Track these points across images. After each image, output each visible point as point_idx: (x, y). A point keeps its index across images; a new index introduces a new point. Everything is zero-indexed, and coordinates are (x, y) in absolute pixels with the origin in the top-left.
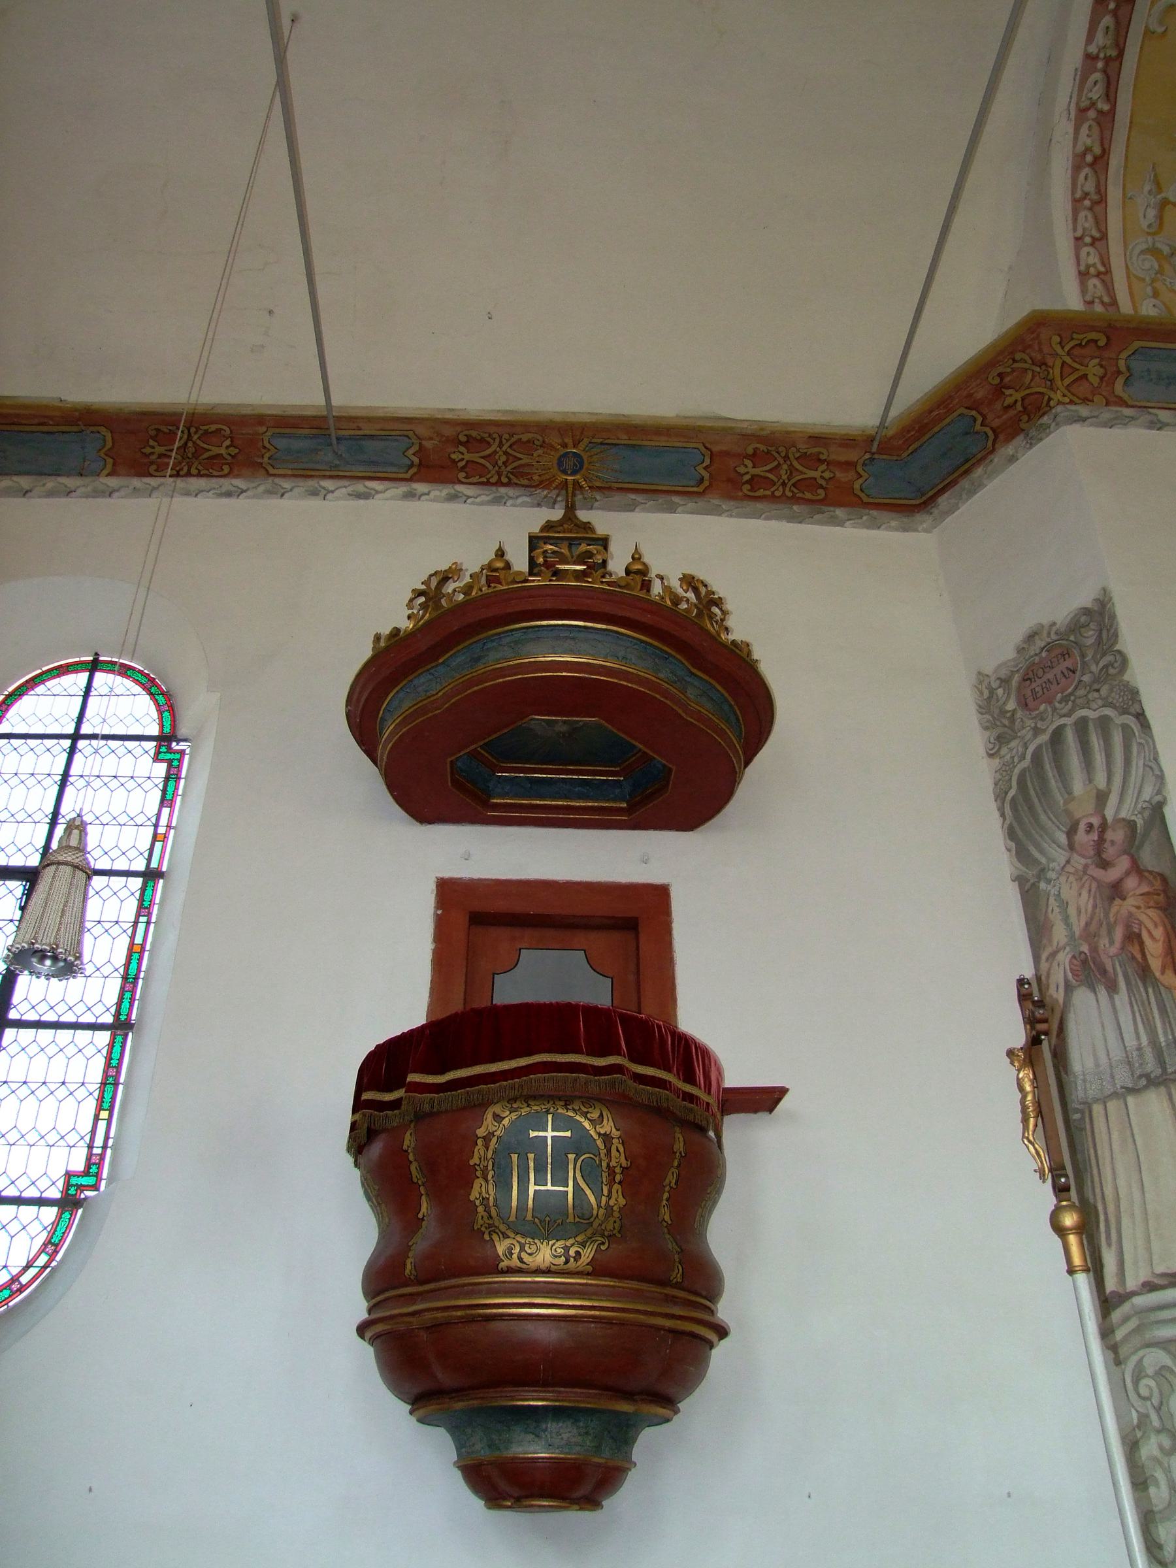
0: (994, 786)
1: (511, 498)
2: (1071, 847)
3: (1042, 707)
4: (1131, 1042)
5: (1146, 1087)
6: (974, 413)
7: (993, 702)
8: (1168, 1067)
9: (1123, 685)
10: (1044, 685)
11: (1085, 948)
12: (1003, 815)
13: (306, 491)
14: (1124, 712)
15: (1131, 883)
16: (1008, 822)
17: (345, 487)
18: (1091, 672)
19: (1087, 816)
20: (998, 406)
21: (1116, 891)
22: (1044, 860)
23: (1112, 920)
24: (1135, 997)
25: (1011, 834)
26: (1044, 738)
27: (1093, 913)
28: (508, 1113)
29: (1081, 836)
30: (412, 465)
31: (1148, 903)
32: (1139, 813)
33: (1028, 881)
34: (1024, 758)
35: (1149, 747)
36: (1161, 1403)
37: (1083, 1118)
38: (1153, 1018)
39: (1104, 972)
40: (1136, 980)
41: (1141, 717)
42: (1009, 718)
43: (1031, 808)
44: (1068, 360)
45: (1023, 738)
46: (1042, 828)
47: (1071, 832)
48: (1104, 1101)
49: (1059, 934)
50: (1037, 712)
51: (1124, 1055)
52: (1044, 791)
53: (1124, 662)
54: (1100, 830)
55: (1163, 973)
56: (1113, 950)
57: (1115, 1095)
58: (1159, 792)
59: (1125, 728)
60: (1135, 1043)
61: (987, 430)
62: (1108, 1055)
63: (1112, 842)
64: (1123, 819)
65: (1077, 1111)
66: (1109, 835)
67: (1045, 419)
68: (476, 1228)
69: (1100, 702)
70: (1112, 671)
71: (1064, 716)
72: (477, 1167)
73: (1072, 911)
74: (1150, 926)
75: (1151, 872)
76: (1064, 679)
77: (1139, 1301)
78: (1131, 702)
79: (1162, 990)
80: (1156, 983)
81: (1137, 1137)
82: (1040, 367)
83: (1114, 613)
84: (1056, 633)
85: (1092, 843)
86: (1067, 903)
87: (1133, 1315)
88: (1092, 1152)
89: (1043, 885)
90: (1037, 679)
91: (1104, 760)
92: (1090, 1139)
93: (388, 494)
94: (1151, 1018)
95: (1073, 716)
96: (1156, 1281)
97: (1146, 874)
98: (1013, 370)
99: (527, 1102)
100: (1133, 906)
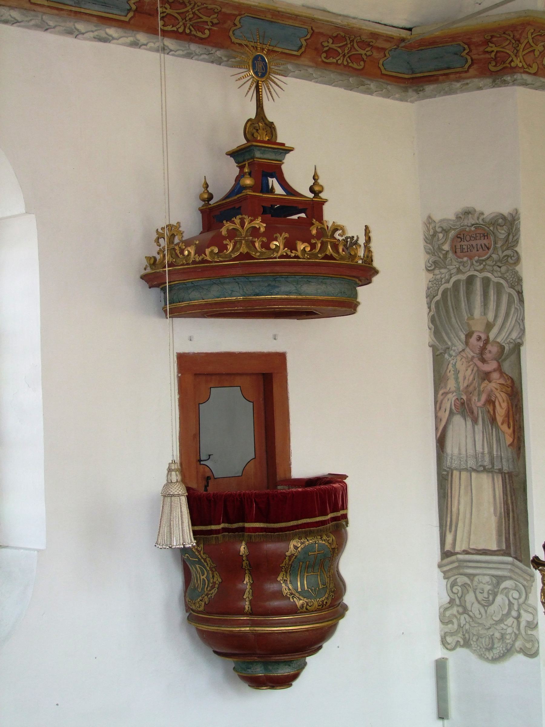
0: (427, 289)
1: (197, 55)
2: (467, 343)
3: (465, 259)
4: (479, 449)
5: (482, 471)
6: (466, 46)
7: (435, 239)
8: (495, 466)
9: (515, 272)
10: (469, 247)
11: (464, 397)
12: (429, 308)
13: (65, 30)
14: (512, 287)
15: (495, 376)
16: (432, 313)
17: (93, 31)
18: (498, 254)
19: (479, 331)
20: (481, 49)
21: (486, 376)
22: (449, 343)
23: (482, 389)
24: (486, 430)
25: (433, 320)
26: (463, 277)
27: (471, 383)
28: (300, 545)
29: (473, 340)
30: (129, 10)
31: (502, 389)
32: (507, 343)
33: (438, 350)
34: (448, 283)
35: (521, 313)
36: (462, 596)
37: (448, 475)
38: (493, 442)
39: (472, 413)
40: (488, 422)
41: (520, 294)
42: (443, 254)
43: (447, 312)
44: (531, 41)
45: (450, 270)
46: (452, 326)
47: (469, 335)
48: (460, 471)
49: (451, 384)
50: (462, 260)
51: (474, 454)
52: (457, 307)
53: (518, 260)
54: (485, 342)
55: (502, 424)
56: (480, 404)
57: (466, 470)
58: (520, 338)
59: (510, 295)
60: (481, 450)
61: (469, 58)
62: (466, 451)
63: (490, 352)
64: (498, 343)
65: (445, 470)
66: (489, 347)
68: (285, 595)
69: (500, 275)
70: (509, 259)
71: (477, 271)
72: (283, 568)
73: (461, 376)
74: (501, 401)
75: (507, 375)
76: (481, 250)
77: (460, 557)
78: (516, 284)
79: (500, 431)
80: (497, 428)
81: (474, 491)
82: (516, 41)
83: (519, 228)
84: (483, 220)
85: (479, 347)
86: (459, 371)
87: (456, 562)
88: (449, 491)
89: (446, 356)
90: (465, 240)
91: (495, 307)
92: (449, 485)
93: (122, 40)
94: (491, 442)
95: (482, 274)
96: (470, 551)
97: (505, 375)
98: (500, 37)
99: (306, 538)
100: (494, 387)
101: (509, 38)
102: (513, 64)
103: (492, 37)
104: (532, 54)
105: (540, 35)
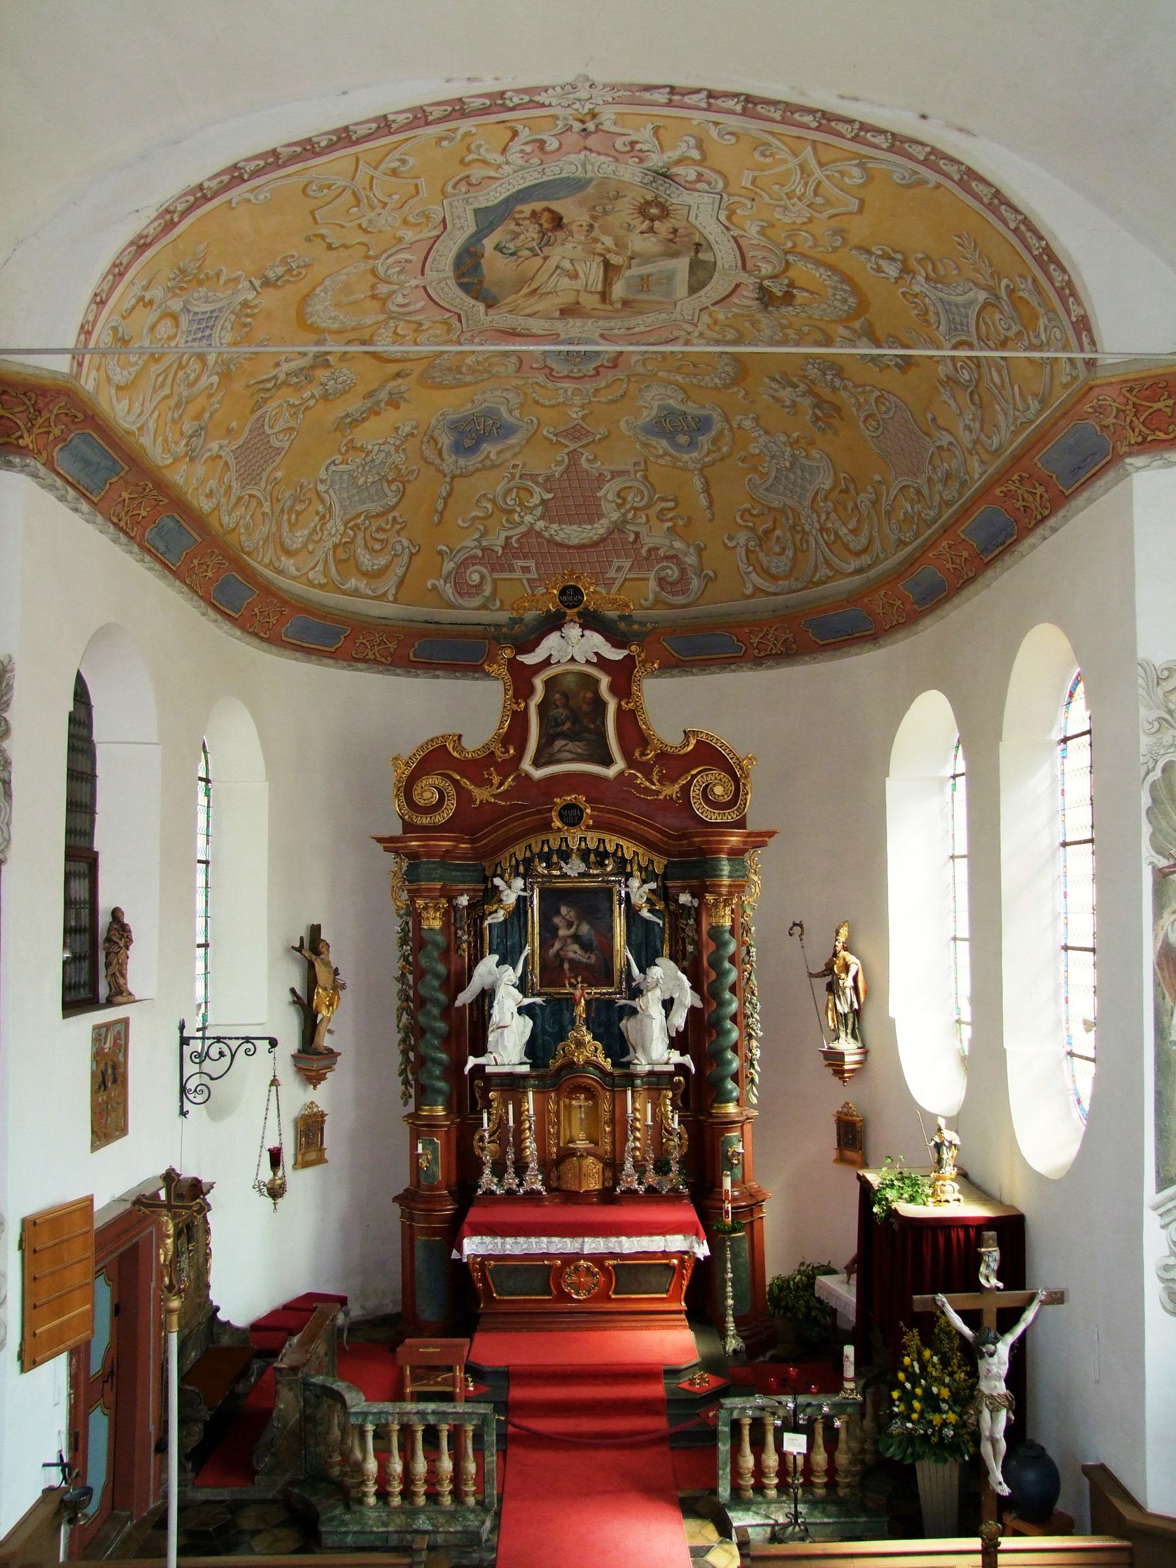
44: (53, 417)
67: (17, 460)
98: (17, 397)
101: (28, 402)
102: (21, 441)
103: (4, 392)
104: (46, 436)
105: (67, 415)
